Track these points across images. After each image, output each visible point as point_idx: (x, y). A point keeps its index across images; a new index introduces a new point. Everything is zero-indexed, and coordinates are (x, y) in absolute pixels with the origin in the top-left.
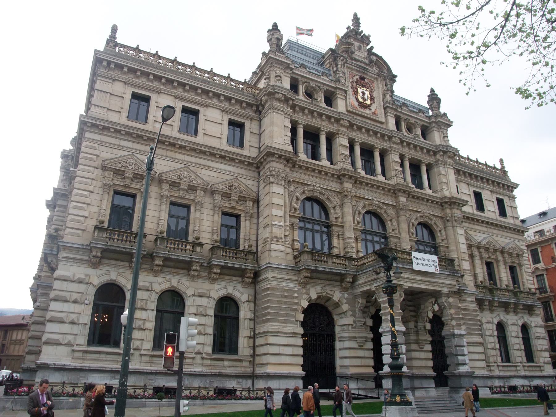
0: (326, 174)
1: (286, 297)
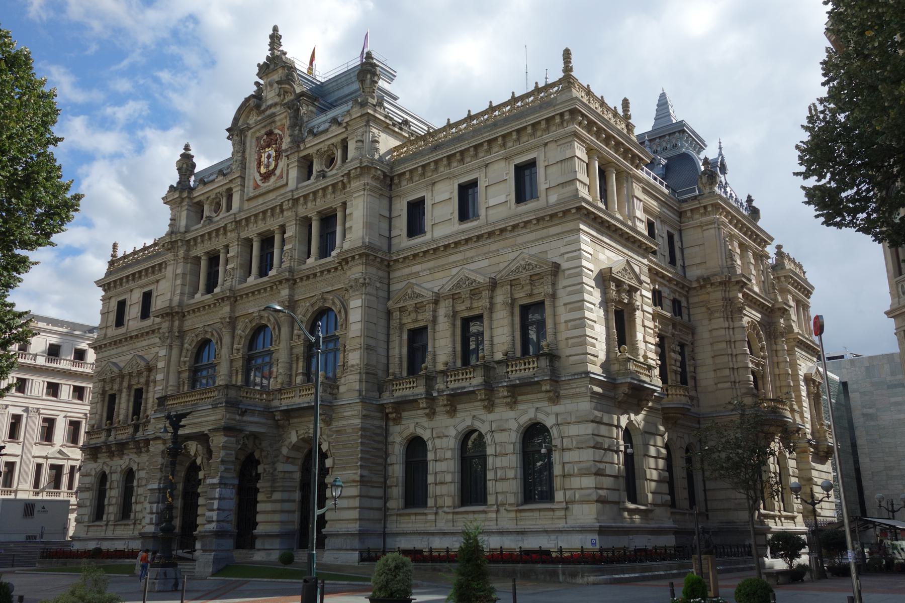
0: (209, 306)
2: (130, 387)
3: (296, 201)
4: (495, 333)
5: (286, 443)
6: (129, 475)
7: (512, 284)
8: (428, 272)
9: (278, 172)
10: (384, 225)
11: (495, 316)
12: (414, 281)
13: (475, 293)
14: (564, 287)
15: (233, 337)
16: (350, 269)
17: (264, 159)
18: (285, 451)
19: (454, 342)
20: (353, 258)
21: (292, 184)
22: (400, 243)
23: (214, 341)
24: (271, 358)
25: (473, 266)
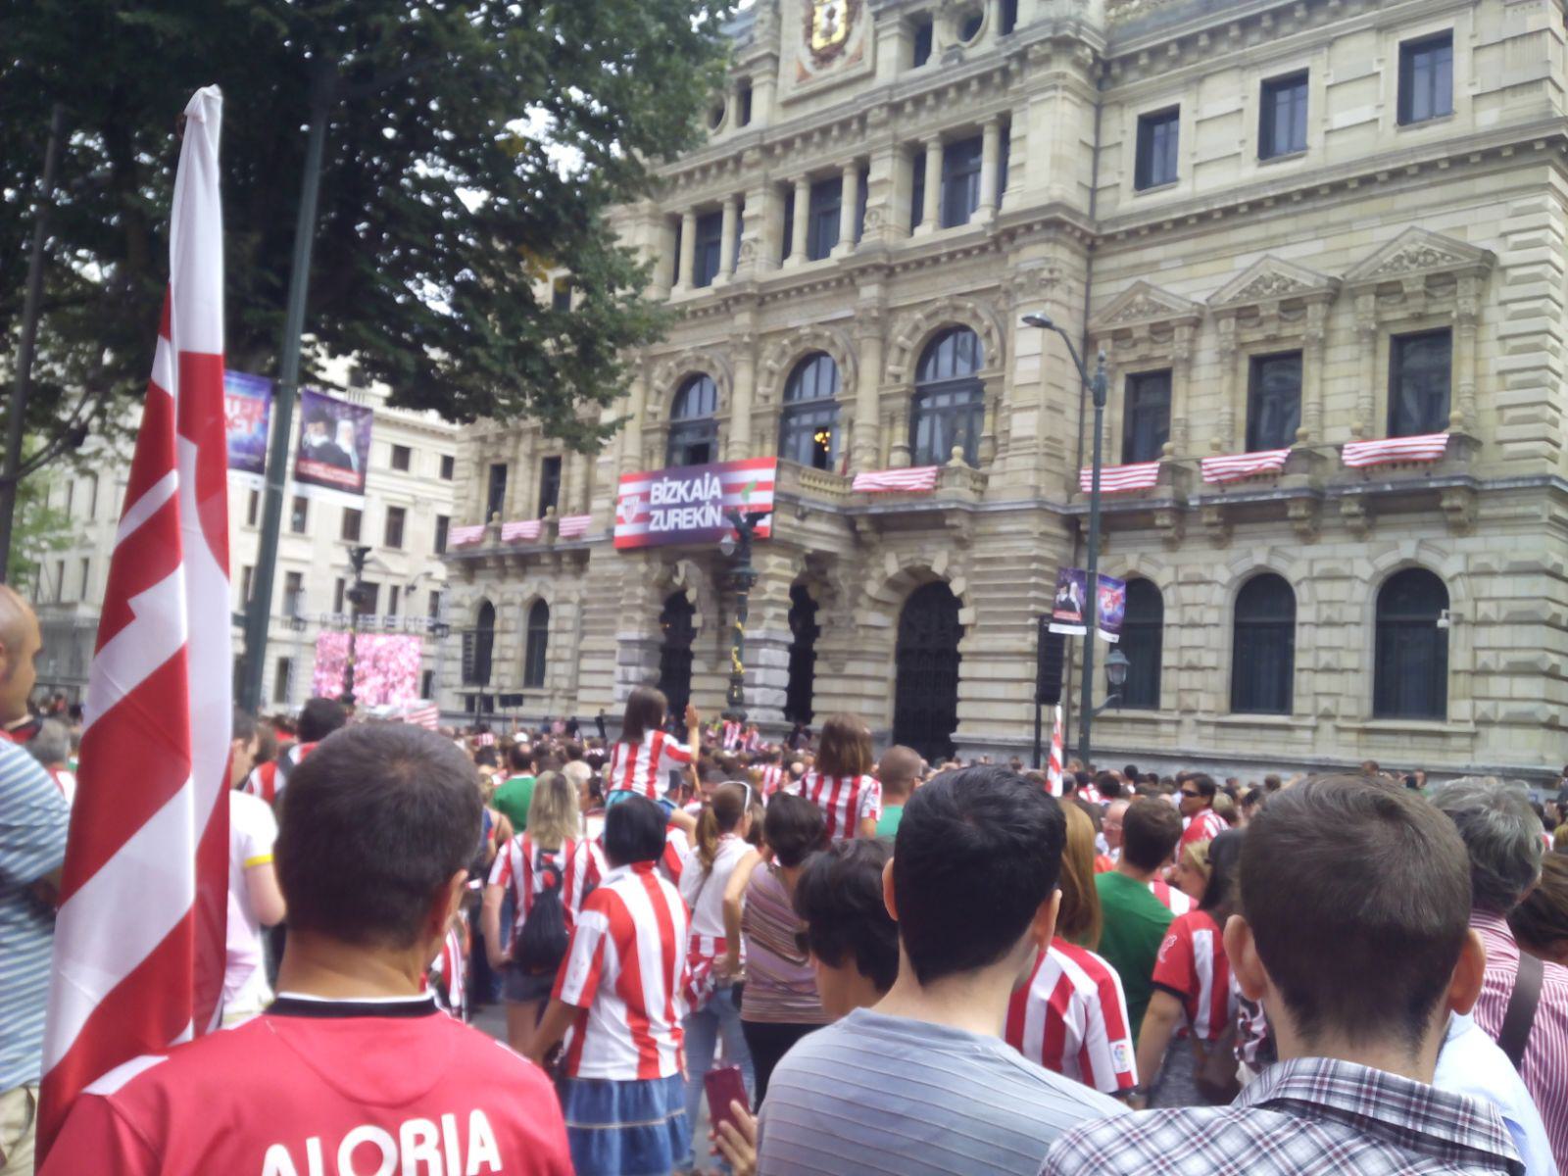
0: (705, 311)
1: (607, 589)
2: (532, 456)
3: (896, 109)
4: (1330, 388)
5: (876, 573)
6: (538, 610)
7: (1387, 291)
8: (1180, 263)
9: (851, 48)
10: (1085, 162)
11: (1332, 355)
12: (1146, 279)
13: (1293, 307)
14: (1503, 303)
15: (756, 373)
16: (1017, 250)
17: (820, 18)
18: (873, 588)
19: (1233, 404)
20: (1029, 228)
21: (885, 75)
22: (1117, 201)
23: (714, 377)
24: (831, 416)
25: (1285, 253)
